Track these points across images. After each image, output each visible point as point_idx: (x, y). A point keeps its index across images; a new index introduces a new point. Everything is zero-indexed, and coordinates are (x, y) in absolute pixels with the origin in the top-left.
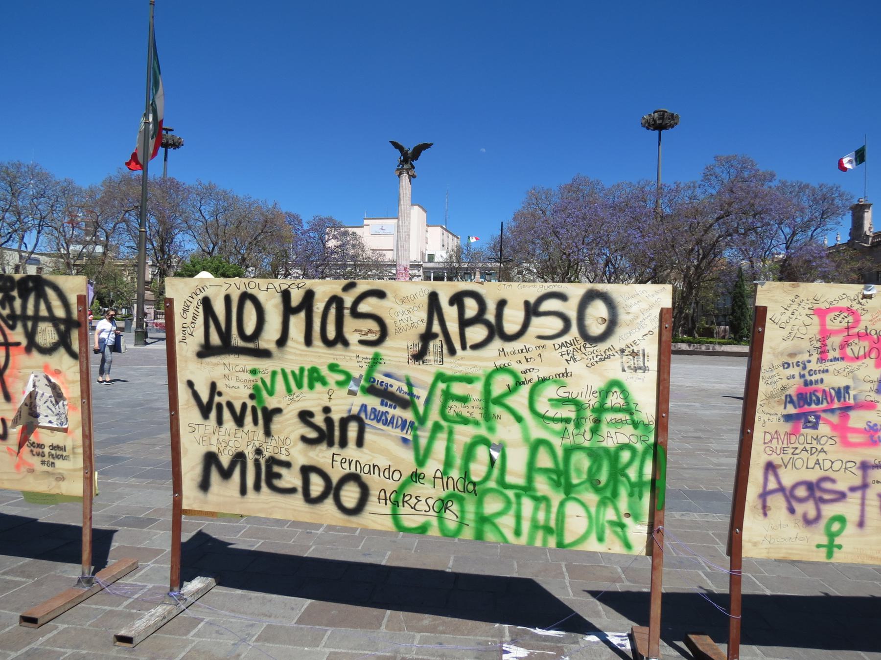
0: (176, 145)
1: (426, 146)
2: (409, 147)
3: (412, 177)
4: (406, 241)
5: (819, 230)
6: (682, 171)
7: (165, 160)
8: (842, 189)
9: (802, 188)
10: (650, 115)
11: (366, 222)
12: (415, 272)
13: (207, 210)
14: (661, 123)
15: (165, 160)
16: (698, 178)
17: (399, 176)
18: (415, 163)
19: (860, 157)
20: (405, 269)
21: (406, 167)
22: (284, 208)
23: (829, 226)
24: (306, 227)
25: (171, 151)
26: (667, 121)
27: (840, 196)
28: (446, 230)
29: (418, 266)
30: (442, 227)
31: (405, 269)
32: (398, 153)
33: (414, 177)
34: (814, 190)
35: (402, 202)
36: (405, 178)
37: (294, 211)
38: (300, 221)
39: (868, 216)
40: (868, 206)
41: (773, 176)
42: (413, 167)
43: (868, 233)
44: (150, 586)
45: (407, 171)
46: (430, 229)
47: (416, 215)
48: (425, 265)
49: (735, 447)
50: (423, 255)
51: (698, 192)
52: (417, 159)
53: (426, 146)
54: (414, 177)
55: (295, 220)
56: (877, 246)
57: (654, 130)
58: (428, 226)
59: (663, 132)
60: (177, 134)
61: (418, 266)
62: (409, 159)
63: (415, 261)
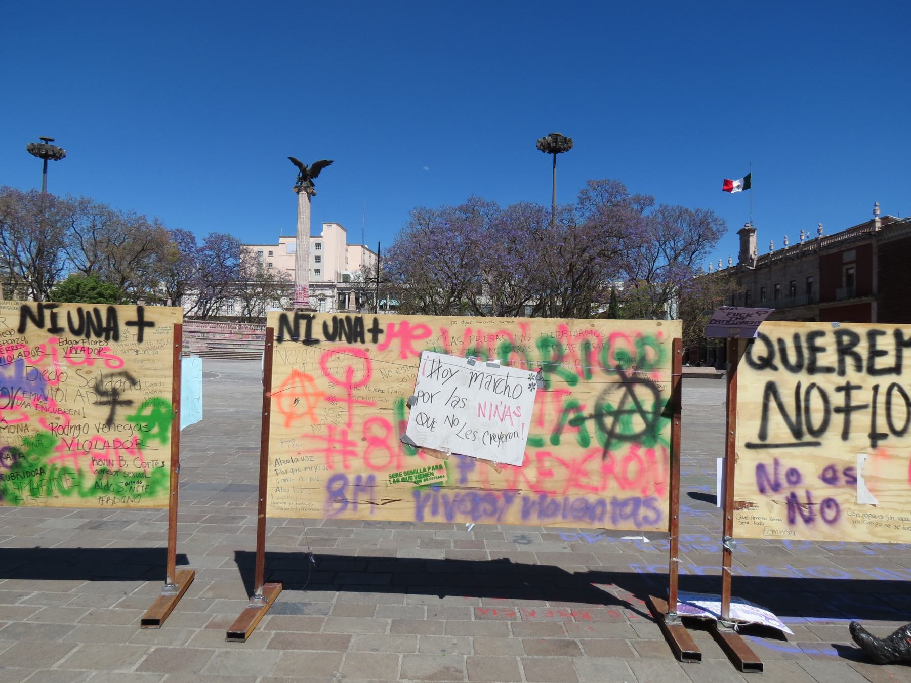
0: (58, 156)
1: (326, 163)
2: (309, 164)
3: (311, 195)
4: (304, 261)
5: (697, 253)
6: (559, 195)
7: (45, 171)
8: (715, 215)
9: (682, 212)
10: (544, 138)
11: (281, 240)
12: (328, 293)
13: (84, 223)
14: (555, 147)
15: (45, 171)
16: (575, 202)
17: (298, 193)
18: (314, 180)
19: (747, 185)
20: (304, 289)
21: (304, 184)
22: (170, 225)
23: (707, 249)
24: (200, 244)
25: (51, 162)
26: (560, 145)
27: (715, 220)
28: (368, 250)
29: (332, 287)
30: (363, 247)
31: (304, 289)
32: (297, 169)
33: (314, 195)
34: (691, 214)
35: (300, 221)
36: (303, 196)
37: (186, 229)
38: (193, 239)
39: (753, 240)
40: (753, 231)
41: (651, 201)
42: (313, 185)
43: (753, 257)
44: (10, 622)
45: (306, 188)
46: (350, 248)
47: (332, 234)
48: (339, 285)
49: (259, 445)
50: (338, 275)
51: (576, 215)
52: (316, 176)
53: (326, 163)
54: (314, 195)
55: (187, 239)
56: (760, 269)
57: (550, 152)
58: (348, 245)
59: (558, 155)
60: (57, 145)
61: (332, 287)
62: (308, 176)
63: (330, 282)
